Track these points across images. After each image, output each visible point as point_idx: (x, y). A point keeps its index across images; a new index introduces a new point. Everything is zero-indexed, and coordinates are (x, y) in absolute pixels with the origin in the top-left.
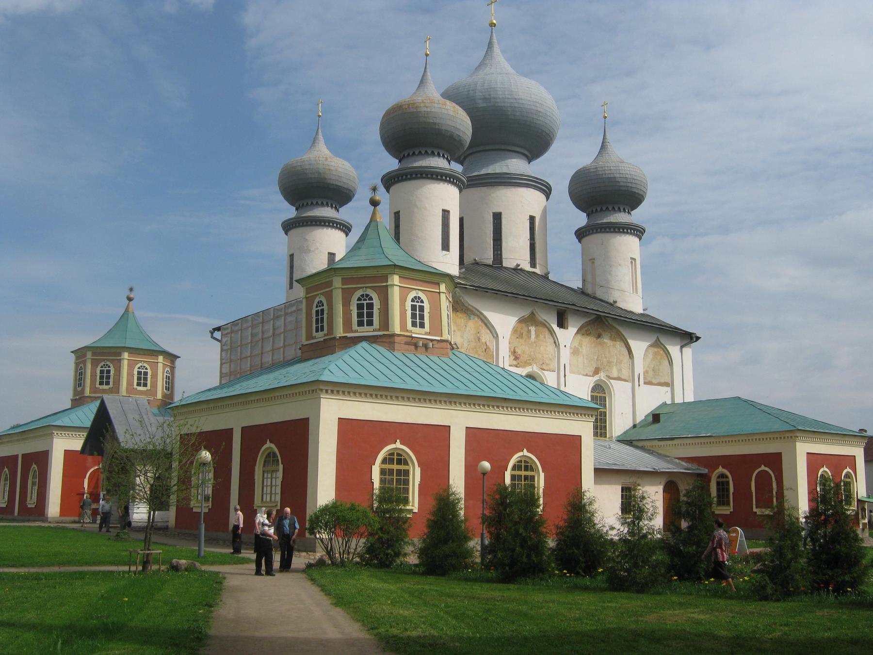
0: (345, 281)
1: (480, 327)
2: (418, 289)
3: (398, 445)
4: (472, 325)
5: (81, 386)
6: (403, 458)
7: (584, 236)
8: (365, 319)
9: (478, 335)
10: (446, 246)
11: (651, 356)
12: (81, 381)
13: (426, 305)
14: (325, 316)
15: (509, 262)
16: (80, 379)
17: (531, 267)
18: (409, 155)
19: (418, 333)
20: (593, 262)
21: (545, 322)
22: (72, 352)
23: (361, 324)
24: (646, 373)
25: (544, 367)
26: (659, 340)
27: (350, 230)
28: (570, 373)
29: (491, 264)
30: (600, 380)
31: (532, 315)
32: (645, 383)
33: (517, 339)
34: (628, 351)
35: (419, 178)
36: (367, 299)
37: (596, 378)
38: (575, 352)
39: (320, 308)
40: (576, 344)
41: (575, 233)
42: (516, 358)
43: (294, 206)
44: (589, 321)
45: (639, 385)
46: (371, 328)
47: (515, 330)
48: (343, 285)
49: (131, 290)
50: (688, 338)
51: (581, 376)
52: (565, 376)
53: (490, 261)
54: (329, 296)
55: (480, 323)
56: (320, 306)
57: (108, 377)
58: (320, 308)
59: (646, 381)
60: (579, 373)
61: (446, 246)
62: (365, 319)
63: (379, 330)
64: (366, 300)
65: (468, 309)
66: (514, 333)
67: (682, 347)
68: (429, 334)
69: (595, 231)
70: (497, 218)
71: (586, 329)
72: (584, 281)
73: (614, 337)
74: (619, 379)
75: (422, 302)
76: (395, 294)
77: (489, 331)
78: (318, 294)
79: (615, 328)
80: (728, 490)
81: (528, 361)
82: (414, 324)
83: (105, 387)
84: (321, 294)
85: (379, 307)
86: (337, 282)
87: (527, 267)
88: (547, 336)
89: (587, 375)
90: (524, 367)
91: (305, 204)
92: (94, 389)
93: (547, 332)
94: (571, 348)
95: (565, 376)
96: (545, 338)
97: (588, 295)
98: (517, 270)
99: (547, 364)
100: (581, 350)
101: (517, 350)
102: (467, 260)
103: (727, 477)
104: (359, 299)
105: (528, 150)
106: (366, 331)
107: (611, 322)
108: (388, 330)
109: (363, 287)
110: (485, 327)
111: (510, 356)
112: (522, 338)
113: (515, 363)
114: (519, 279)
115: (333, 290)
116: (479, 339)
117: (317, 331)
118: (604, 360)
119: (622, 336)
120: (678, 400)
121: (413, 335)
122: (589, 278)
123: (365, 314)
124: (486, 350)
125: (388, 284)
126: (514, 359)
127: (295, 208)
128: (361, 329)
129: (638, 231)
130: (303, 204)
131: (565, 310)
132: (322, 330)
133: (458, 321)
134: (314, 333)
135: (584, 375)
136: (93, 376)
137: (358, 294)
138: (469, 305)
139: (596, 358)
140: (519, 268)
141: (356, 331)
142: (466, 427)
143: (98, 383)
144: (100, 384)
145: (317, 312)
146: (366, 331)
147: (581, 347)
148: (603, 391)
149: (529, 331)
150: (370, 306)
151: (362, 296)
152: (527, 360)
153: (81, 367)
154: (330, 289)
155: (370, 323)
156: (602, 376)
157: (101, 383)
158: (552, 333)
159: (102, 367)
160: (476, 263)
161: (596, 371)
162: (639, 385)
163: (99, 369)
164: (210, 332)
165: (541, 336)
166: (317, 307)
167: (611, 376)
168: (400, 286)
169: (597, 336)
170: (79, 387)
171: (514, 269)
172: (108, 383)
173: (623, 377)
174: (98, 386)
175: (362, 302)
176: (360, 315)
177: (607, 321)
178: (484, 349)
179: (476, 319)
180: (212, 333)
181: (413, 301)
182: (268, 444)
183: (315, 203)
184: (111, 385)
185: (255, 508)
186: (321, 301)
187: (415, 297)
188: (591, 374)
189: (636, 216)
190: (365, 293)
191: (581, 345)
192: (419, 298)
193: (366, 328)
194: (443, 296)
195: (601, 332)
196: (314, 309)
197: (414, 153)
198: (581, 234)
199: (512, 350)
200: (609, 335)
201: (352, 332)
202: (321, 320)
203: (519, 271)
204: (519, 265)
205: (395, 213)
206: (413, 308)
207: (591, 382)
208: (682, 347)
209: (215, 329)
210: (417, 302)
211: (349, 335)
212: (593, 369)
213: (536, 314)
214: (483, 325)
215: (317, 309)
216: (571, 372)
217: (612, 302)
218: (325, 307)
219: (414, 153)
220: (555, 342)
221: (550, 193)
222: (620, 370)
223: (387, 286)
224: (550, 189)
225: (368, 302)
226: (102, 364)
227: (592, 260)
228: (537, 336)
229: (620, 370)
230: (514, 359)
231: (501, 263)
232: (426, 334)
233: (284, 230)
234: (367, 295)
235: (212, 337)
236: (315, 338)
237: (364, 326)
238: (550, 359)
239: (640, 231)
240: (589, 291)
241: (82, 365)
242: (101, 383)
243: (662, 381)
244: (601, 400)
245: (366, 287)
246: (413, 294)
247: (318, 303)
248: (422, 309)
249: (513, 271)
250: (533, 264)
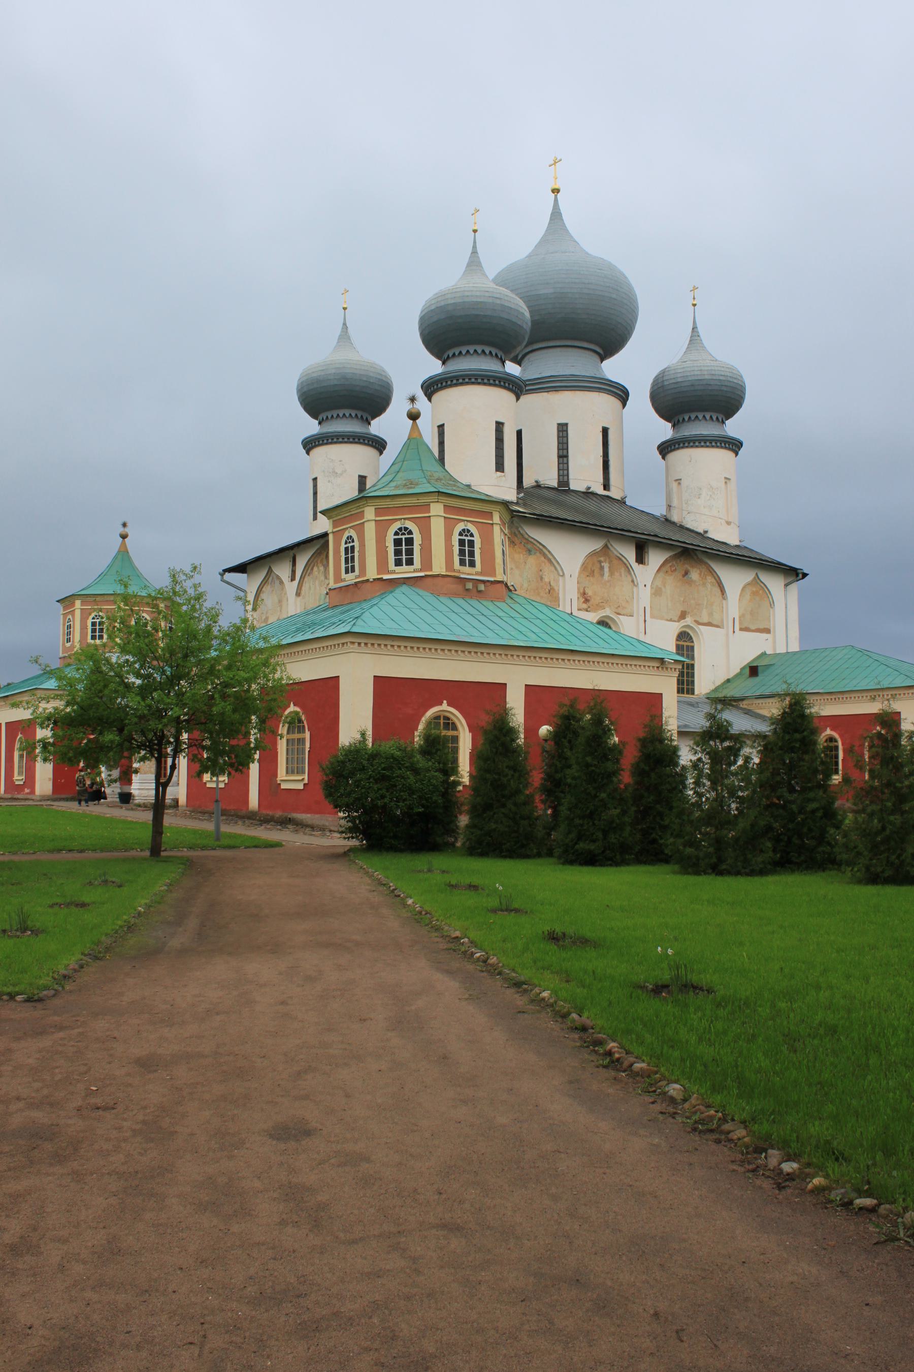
0: (378, 512)
1: (543, 564)
2: (467, 521)
3: (445, 706)
4: (532, 560)
5: (70, 641)
6: (450, 722)
7: (669, 452)
8: (404, 557)
9: (541, 573)
10: (500, 467)
11: (748, 596)
12: (70, 635)
13: (477, 539)
14: (356, 554)
15: (576, 484)
16: (69, 633)
17: (605, 489)
18: (454, 355)
19: (466, 572)
20: (679, 484)
21: (620, 556)
22: (58, 601)
23: (398, 563)
24: (742, 617)
25: (620, 611)
26: (758, 578)
27: (384, 448)
28: (651, 617)
29: (556, 486)
30: (688, 626)
31: (606, 546)
32: (741, 629)
33: (588, 578)
34: (722, 591)
35: (467, 383)
36: (406, 533)
37: (683, 623)
38: (657, 592)
39: (349, 545)
40: (658, 583)
41: (659, 447)
42: (587, 601)
43: (316, 418)
44: (676, 554)
45: (734, 632)
46: (411, 568)
47: (584, 567)
48: (376, 515)
49: (124, 525)
50: (793, 574)
51: (664, 622)
52: (645, 621)
53: (555, 484)
54: (360, 529)
55: (543, 558)
56: (350, 542)
58: (349, 545)
59: (743, 627)
60: (662, 618)
61: (500, 466)
62: (404, 557)
63: (421, 570)
64: (403, 534)
65: (528, 542)
66: (584, 570)
67: (786, 585)
68: (481, 574)
69: (681, 445)
70: (563, 429)
71: (670, 564)
72: (669, 507)
73: (704, 574)
74: (709, 624)
75: (472, 535)
76: (437, 527)
77: (553, 569)
78: (347, 528)
79: (706, 563)
80: (837, 757)
81: (601, 604)
82: (462, 563)
84: (350, 527)
85: (421, 543)
86: (369, 513)
87: (600, 491)
88: (623, 575)
89: (671, 620)
90: (595, 610)
91: (329, 417)
93: (623, 570)
94: (652, 588)
95: (645, 621)
96: (621, 575)
97: (674, 523)
98: (588, 494)
99: (624, 608)
100: (663, 589)
101: (587, 591)
102: (528, 482)
103: (836, 741)
104: (396, 534)
105: (601, 347)
106: (405, 571)
107: (700, 555)
108: (431, 570)
109: (401, 519)
110: (547, 564)
111: (578, 598)
112: (593, 576)
113: (585, 606)
114: (591, 505)
115: (366, 524)
116: (542, 578)
117: (347, 572)
118: (692, 602)
119: (714, 573)
120: (781, 649)
121: (462, 576)
122: (675, 503)
124: (549, 591)
125: (430, 514)
126: (584, 602)
127: (317, 422)
128: (398, 569)
129: (734, 445)
130: (327, 417)
131: (646, 542)
132: (353, 570)
133: (516, 556)
134: (344, 575)
135: (667, 620)
137: (396, 526)
138: (529, 536)
139: (682, 599)
140: (590, 491)
141: (394, 572)
142: (526, 685)
143: (89, 637)
144: (92, 639)
145: (346, 549)
146: (405, 571)
147: (665, 587)
148: (691, 639)
149: (602, 568)
150: (410, 542)
151: (400, 529)
152: (599, 603)
153: (69, 619)
154: (362, 521)
155: (410, 562)
156: (689, 621)
158: (628, 569)
159: (93, 618)
160: (538, 486)
161: (683, 616)
162: (734, 632)
164: (220, 574)
165: (617, 574)
166: (346, 543)
167: (701, 621)
168: (445, 517)
169: (683, 573)
170: (67, 642)
171: (583, 493)
173: (715, 623)
174: (90, 641)
175: (400, 537)
176: (398, 553)
177: (696, 555)
178: (547, 590)
179: (538, 554)
180: (222, 575)
181: (460, 534)
182: (292, 708)
183: (341, 415)
184: (105, 640)
185: (279, 782)
186: (351, 537)
187: (464, 530)
188: (676, 619)
189: (733, 427)
190: (403, 526)
191: (664, 584)
192: (468, 531)
193: (405, 567)
194: (497, 529)
195: (689, 568)
196: (343, 546)
197: (460, 353)
198: (665, 449)
199: (582, 591)
200: (698, 572)
201: (389, 572)
202: (349, 560)
203: (591, 496)
204: (589, 488)
205: (439, 427)
206: (462, 543)
207: (675, 628)
208: (786, 585)
209: (225, 571)
210: (466, 536)
211: (385, 577)
212: (679, 613)
213: (610, 546)
214: (546, 561)
215: (346, 546)
216: (652, 616)
217: (702, 532)
218: (356, 544)
219: (460, 353)
220: (633, 581)
221: (628, 399)
222: (711, 614)
223: (430, 517)
224: (627, 394)
225: (407, 536)
227: (678, 481)
228: (612, 573)
229: (711, 614)
230: (584, 602)
231: (567, 484)
232: (477, 574)
233: (304, 448)
234: (406, 529)
235: (223, 580)
236: (342, 580)
237: (402, 565)
238: (627, 602)
239: (734, 444)
240: (675, 518)
241: (70, 617)
243: (762, 627)
244: (688, 650)
245: (405, 519)
246: (460, 527)
247: (348, 538)
248: (471, 544)
249: (582, 495)
250: (606, 487)
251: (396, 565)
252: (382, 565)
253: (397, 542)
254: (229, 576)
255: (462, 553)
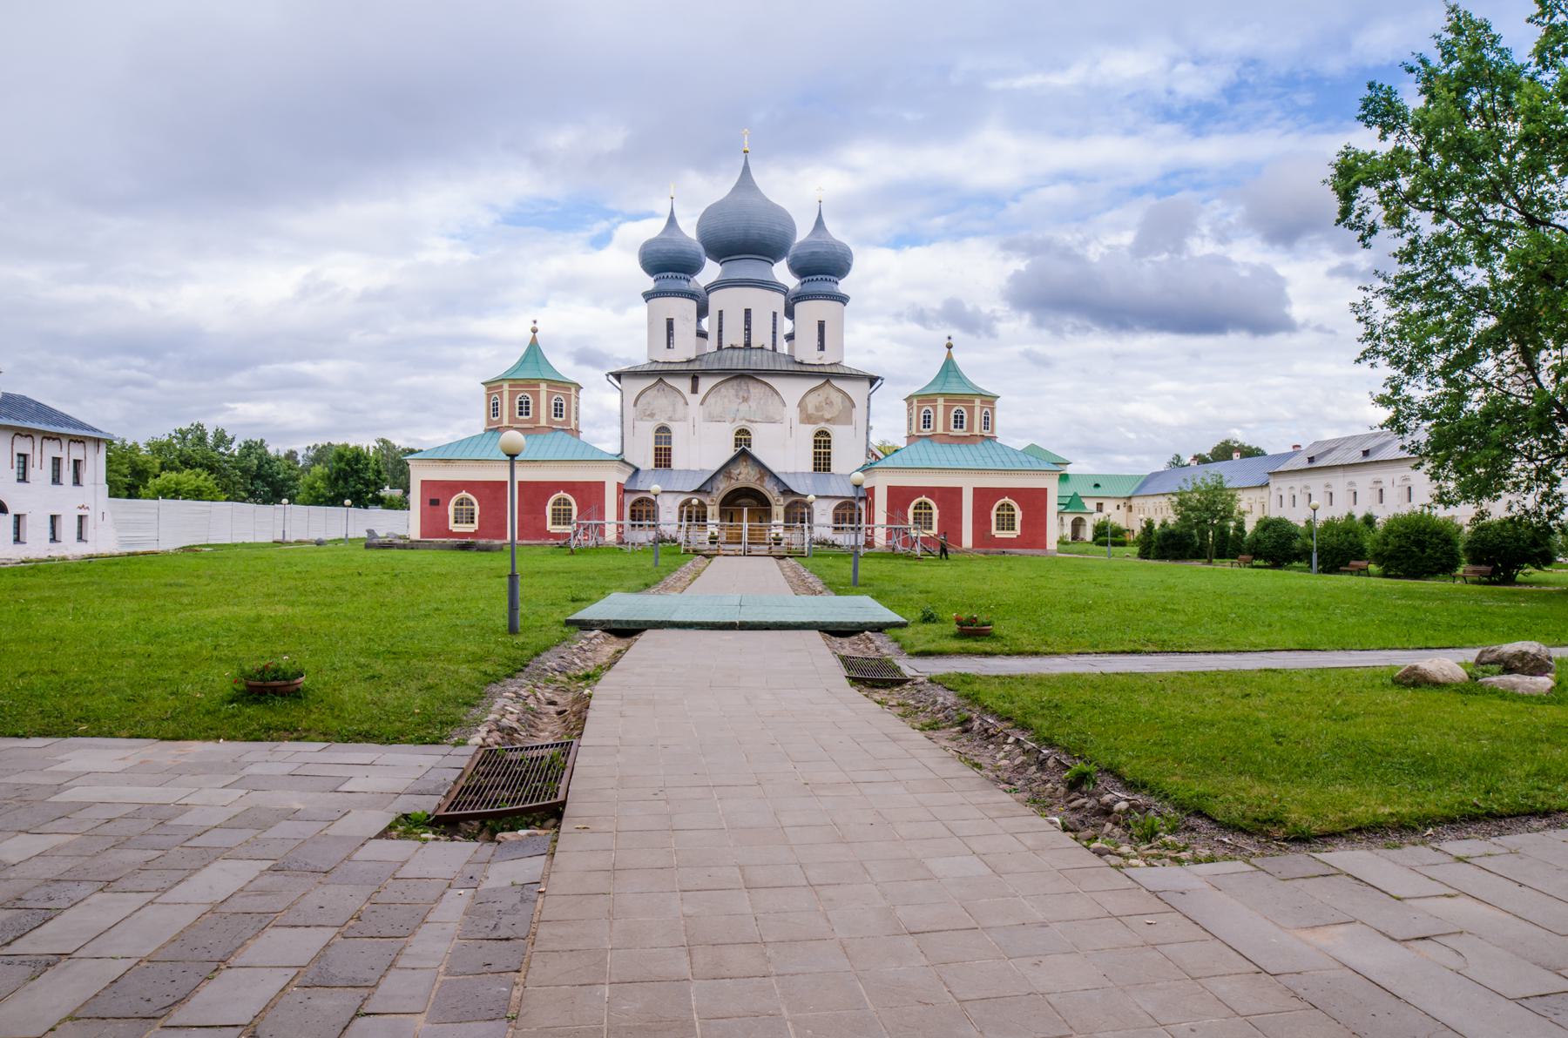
23: (956, 427)
57: (561, 410)
83: (558, 419)
92: (549, 420)
106: (958, 432)
123: (959, 420)
127: (652, 279)
136: (549, 406)
137: (955, 409)
146: (958, 432)
150: (962, 417)
155: (961, 427)
157: (556, 415)
163: (553, 402)
172: (561, 416)
193: (958, 430)
211: (951, 434)
226: (555, 397)
242: (556, 415)
251: (956, 427)
252: (946, 427)
253: (956, 417)
254: (611, 377)
255: (956, 422)
